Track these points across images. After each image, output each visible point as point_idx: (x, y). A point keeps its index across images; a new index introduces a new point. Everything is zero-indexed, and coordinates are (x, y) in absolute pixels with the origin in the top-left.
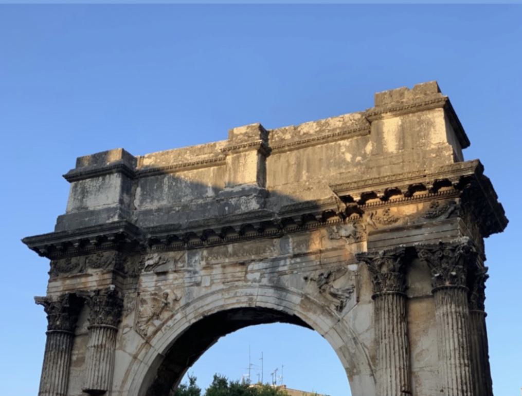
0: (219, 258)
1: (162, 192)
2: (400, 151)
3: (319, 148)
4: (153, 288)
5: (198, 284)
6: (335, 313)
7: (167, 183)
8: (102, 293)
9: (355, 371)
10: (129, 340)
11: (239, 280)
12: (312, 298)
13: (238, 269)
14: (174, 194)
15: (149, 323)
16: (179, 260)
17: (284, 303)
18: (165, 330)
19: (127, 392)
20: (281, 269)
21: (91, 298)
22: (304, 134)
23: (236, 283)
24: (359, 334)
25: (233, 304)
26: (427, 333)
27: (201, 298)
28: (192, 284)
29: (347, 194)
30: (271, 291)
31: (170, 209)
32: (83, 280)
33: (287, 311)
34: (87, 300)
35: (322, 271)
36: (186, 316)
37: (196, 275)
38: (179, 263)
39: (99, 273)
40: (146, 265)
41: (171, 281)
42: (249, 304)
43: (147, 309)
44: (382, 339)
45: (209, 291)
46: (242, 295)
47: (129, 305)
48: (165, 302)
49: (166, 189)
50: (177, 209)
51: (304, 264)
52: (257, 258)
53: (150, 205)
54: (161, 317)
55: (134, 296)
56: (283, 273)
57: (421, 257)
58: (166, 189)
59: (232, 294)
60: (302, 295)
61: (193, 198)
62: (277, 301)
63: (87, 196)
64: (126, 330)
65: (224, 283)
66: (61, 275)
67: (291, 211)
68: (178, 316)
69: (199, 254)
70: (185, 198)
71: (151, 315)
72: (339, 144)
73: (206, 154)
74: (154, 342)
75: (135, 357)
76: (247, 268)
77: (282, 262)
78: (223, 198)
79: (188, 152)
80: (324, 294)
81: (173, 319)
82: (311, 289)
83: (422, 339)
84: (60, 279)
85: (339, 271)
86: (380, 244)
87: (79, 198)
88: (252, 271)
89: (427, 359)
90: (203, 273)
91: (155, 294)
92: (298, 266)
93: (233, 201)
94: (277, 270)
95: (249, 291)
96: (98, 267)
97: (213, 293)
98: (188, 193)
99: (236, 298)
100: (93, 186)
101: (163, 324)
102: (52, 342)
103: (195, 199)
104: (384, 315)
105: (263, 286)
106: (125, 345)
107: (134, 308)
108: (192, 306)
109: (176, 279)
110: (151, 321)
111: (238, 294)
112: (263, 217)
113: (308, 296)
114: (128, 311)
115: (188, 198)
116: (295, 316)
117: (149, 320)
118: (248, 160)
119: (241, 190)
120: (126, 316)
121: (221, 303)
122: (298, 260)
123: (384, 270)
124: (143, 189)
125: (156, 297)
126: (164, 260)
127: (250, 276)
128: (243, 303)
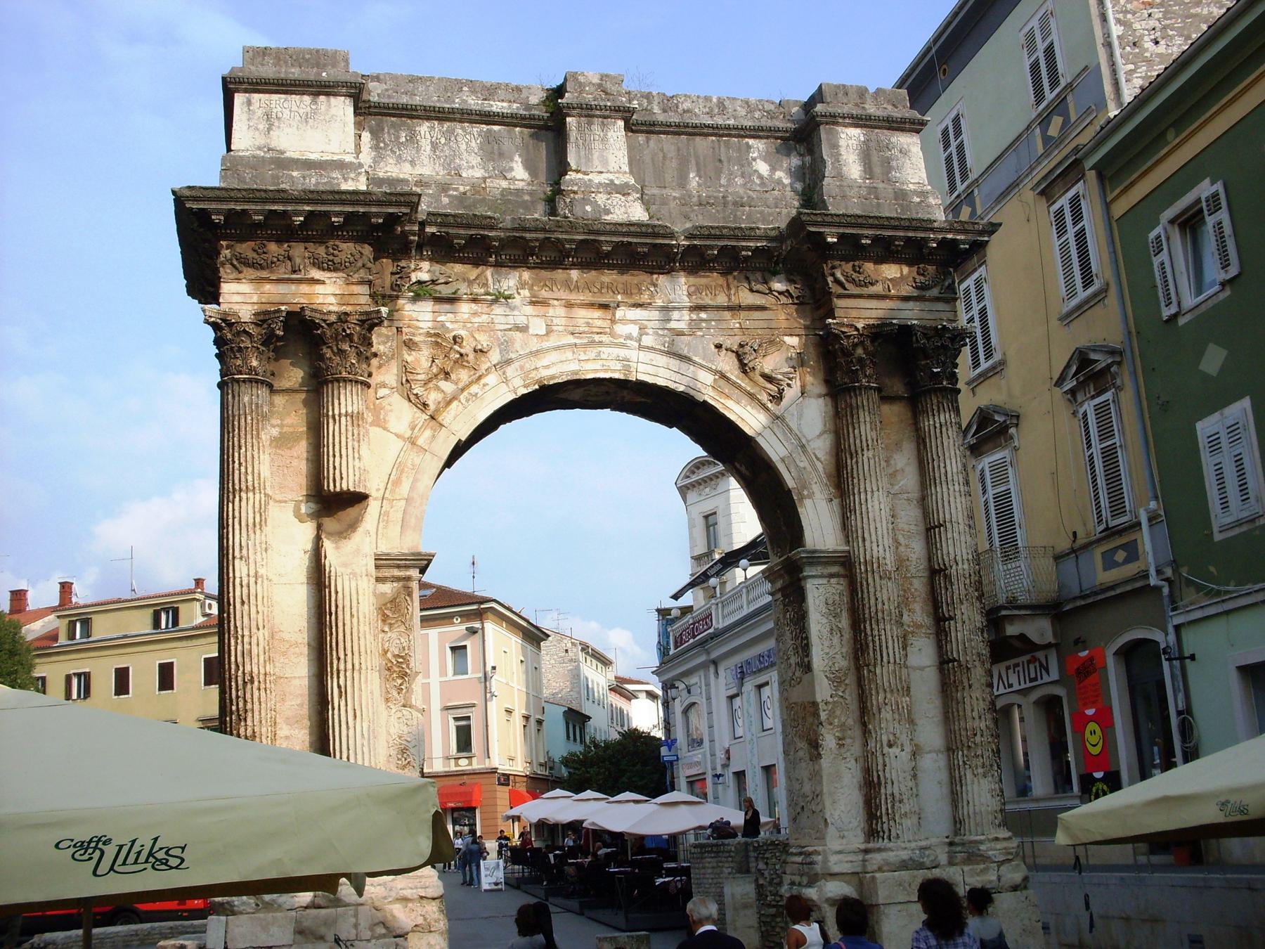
0: (554, 288)
1: (418, 149)
2: (867, 181)
3: (713, 141)
4: (430, 324)
5: (523, 329)
6: (769, 405)
7: (428, 136)
8: (353, 319)
9: (805, 493)
10: (391, 411)
11: (601, 333)
12: (733, 378)
13: (597, 313)
14: (445, 160)
15: (431, 385)
16: (474, 280)
17: (685, 380)
18: (468, 400)
19: (403, 503)
20: (673, 325)
21: (330, 325)
22: (684, 111)
23: (597, 338)
24: (808, 441)
25: (596, 371)
26: (900, 447)
27: (536, 353)
28: (509, 327)
29: (821, 230)
30: (662, 360)
31: (444, 188)
32: (305, 288)
33: (692, 393)
34: (322, 327)
35: (744, 338)
36: (506, 381)
37: (516, 313)
38: (476, 286)
39: (340, 282)
40: (414, 280)
41: (466, 316)
42: (625, 374)
43: (421, 359)
44: (863, 450)
45: (546, 345)
46: (610, 358)
47: (382, 348)
48: (463, 351)
49: (426, 145)
50: (462, 189)
51: (713, 323)
52: (631, 301)
53: (396, 170)
54: (453, 376)
55: (390, 334)
56: (680, 333)
57: (917, 341)
58: (426, 145)
59: (592, 353)
60: (716, 372)
61: (487, 175)
62: (677, 378)
63: (279, 127)
64: (382, 392)
65: (573, 334)
66: (250, 273)
67: (709, 237)
68: (492, 379)
69: (514, 276)
70: (470, 171)
71: (435, 370)
72: (747, 143)
73: (503, 101)
74: (447, 417)
75: (413, 442)
76: (614, 315)
77: (676, 315)
78: (575, 188)
79: (465, 89)
80: (751, 374)
81: (483, 381)
82: (728, 364)
83: (895, 456)
84: (252, 281)
85: (771, 342)
86: (854, 313)
87: (261, 127)
88: (624, 321)
89: (902, 483)
90: (529, 310)
91: (437, 335)
92: (704, 325)
93: (601, 199)
94: (669, 326)
95: (623, 353)
96: (335, 270)
97: (557, 348)
98: (474, 163)
99: (601, 362)
100: (291, 111)
101: (463, 390)
102: (246, 399)
103: (490, 177)
104: (864, 416)
105: (648, 348)
106: (384, 419)
107: (394, 355)
108: (516, 365)
109: (475, 314)
110: (434, 381)
111: (603, 356)
112: (656, 235)
113: (728, 375)
114: (381, 356)
115: (479, 173)
116: (705, 402)
117: (430, 380)
118: (609, 134)
119: (607, 182)
120: (380, 367)
121: (574, 366)
122: (703, 315)
123: (860, 351)
124: (376, 134)
125: (439, 340)
126: (450, 277)
127: (620, 329)
128: (614, 371)
